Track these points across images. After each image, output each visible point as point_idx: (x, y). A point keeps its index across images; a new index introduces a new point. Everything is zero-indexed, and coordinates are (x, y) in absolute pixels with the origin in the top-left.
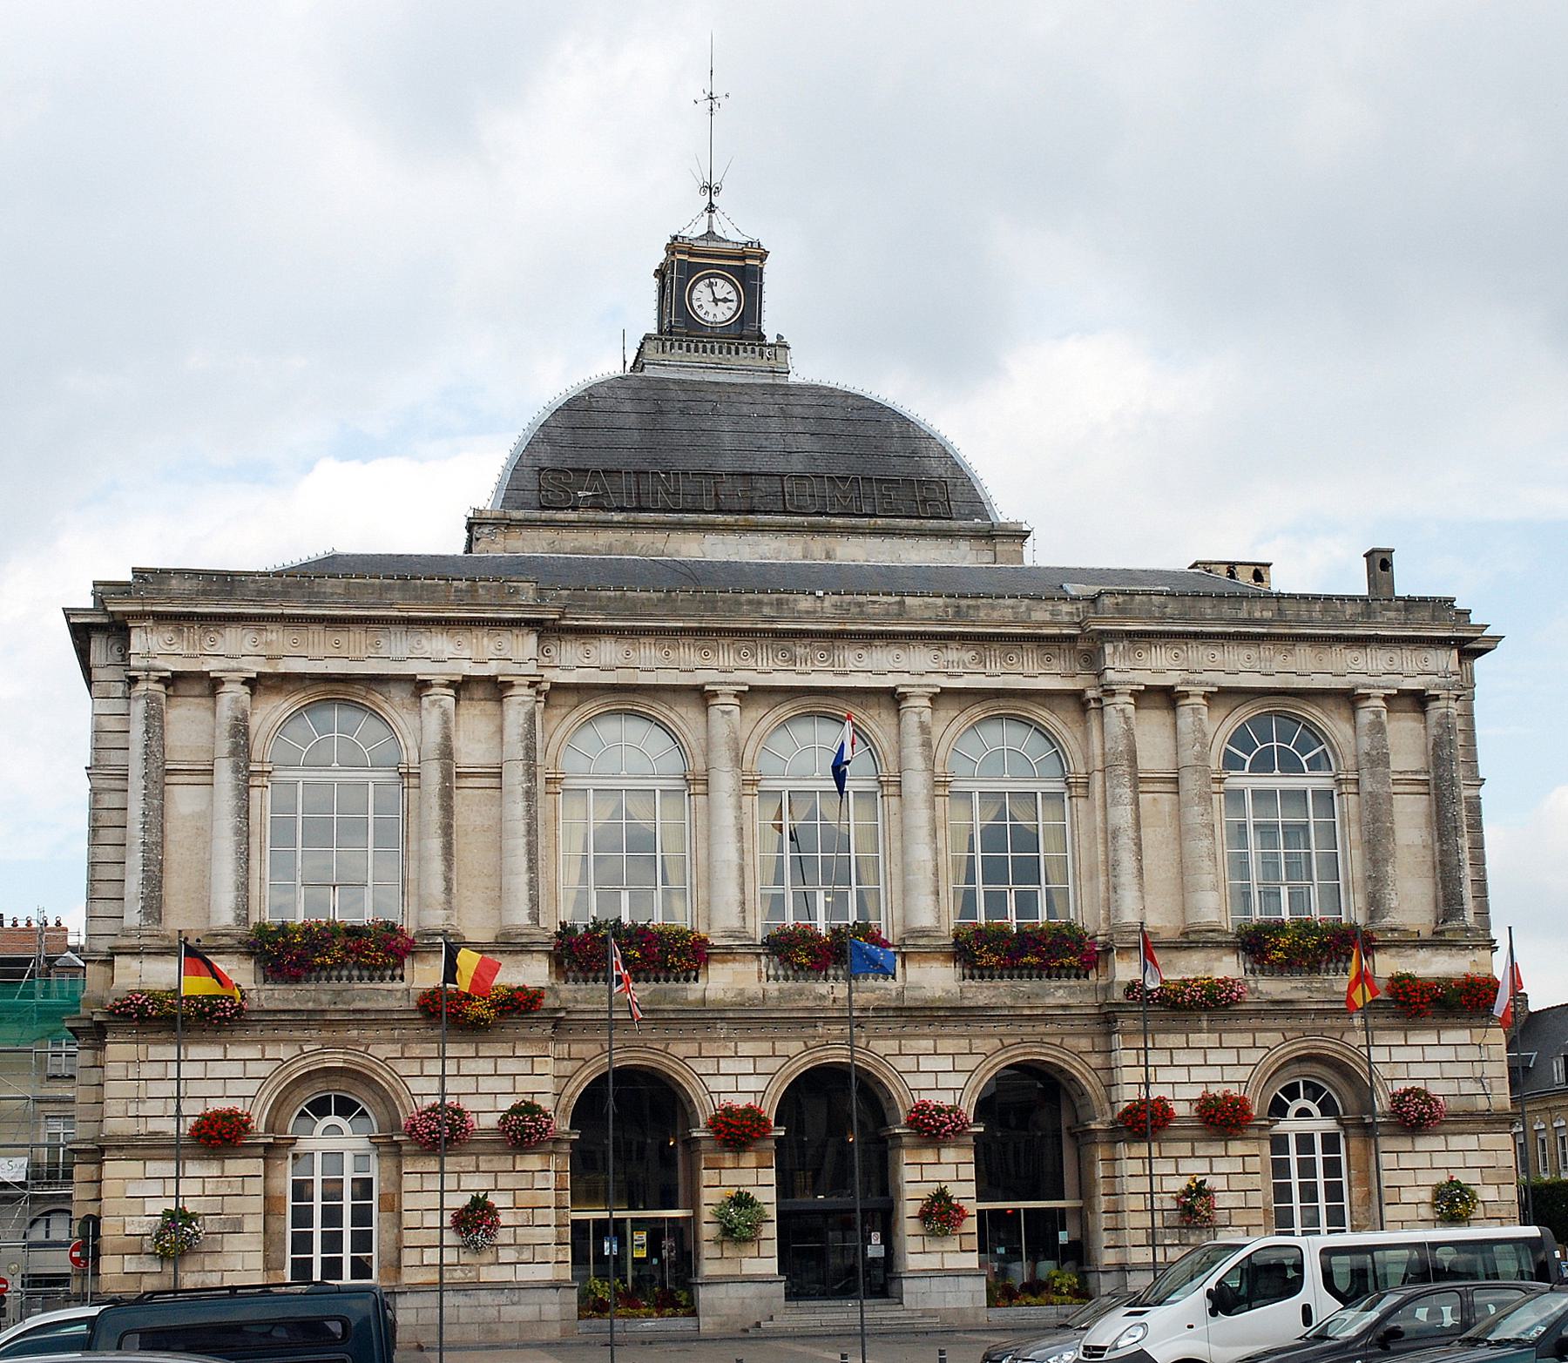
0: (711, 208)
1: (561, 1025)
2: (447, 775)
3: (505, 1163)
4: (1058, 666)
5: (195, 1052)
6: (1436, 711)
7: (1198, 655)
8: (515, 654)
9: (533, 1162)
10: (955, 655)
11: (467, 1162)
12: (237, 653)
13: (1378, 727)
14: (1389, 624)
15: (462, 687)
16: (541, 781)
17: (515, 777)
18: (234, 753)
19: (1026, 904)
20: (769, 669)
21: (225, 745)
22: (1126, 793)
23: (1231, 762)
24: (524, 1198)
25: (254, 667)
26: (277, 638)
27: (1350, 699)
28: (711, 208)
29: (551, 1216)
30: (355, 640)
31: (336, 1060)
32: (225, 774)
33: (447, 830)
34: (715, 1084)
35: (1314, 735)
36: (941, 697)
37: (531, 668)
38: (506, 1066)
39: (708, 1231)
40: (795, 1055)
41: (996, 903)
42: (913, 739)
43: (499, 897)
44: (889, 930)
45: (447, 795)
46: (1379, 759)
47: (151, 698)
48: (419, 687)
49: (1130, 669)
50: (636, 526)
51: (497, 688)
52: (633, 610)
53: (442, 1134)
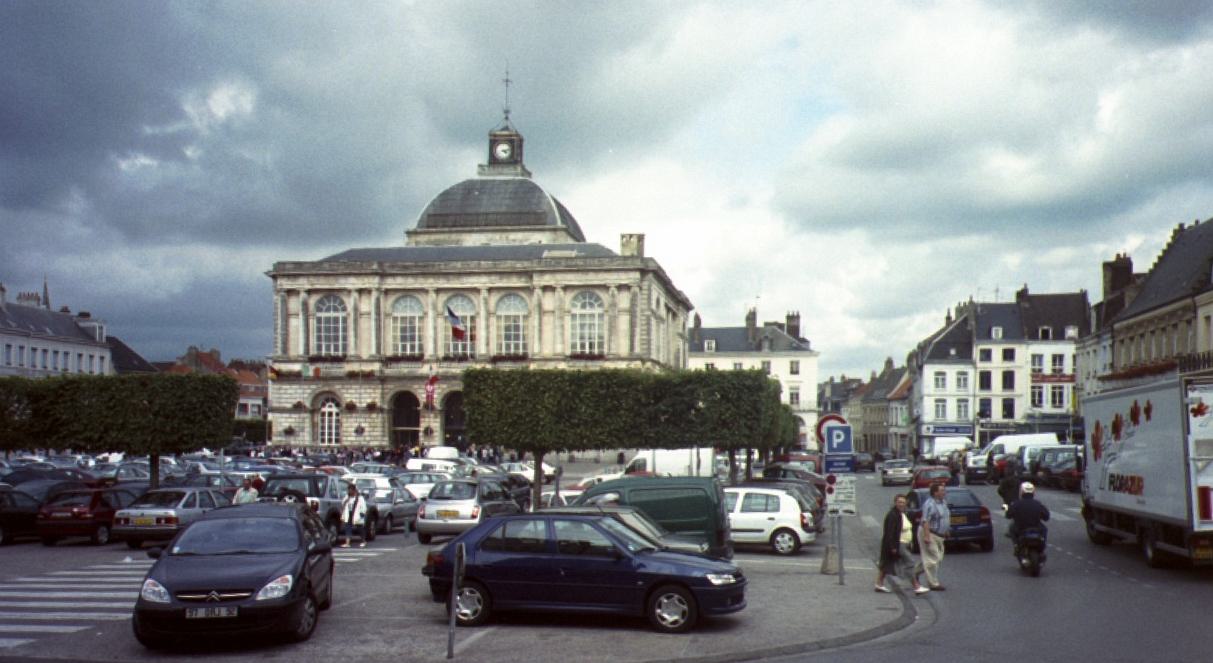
0: (507, 118)
1: (308, 380)
2: (355, 314)
3: (367, 416)
4: (523, 279)
5: (284, 387)
6: (633, 290)
7: (559, 276)
8: (372, 282)
9: (374, 415)
10: (493, 278)
11: (358, 415)
12: (303, 284)
13: (613, 296)
14: (619, 265)
15: (361, 291)
16: (382, 316)
17: (373, 316)
18: (303, 310)
19: (517, 347)
20: (443, 283)
21: (300, 308)
22: (537, 316)
23: (574, 306)
24: (372, 425)
25: (308, 287)
26: (312, 279)
27: (605, 287)
28: (507, 118)
29: (379, 429)
30: (332, 280)
31: (326, 389)
32: (301, 316)
33: (356, 330)
34: (346, 395)
35: (598, 299)
36: (490, 290)
37: (377, 286)
38: (368, 391)
39: (421, 434)
40: (392, 388)
41: (508, 347)
42: (482, 301)
43: (370, 347)
44: (530, 356)
45: (356, 321)
46: (614, 305)
47: (282, 296)
48: (349, 291)
49: (539, 281)
50: (451, 232)
51: (368, 291)
52: (406, 267)
53: (351, 408)
